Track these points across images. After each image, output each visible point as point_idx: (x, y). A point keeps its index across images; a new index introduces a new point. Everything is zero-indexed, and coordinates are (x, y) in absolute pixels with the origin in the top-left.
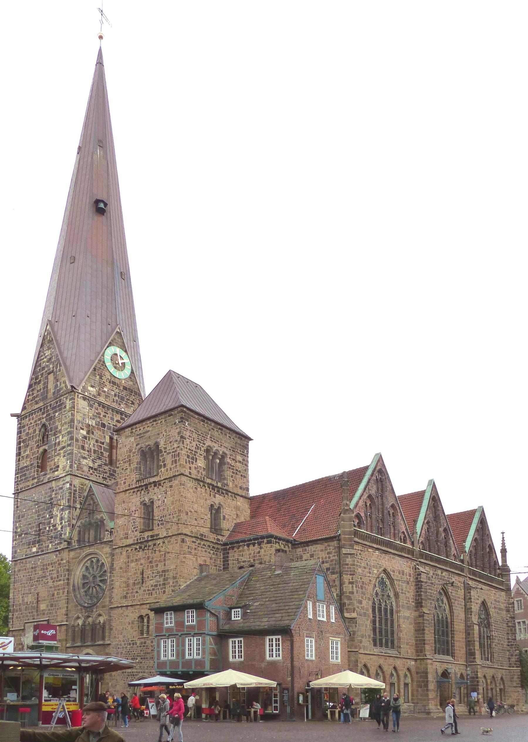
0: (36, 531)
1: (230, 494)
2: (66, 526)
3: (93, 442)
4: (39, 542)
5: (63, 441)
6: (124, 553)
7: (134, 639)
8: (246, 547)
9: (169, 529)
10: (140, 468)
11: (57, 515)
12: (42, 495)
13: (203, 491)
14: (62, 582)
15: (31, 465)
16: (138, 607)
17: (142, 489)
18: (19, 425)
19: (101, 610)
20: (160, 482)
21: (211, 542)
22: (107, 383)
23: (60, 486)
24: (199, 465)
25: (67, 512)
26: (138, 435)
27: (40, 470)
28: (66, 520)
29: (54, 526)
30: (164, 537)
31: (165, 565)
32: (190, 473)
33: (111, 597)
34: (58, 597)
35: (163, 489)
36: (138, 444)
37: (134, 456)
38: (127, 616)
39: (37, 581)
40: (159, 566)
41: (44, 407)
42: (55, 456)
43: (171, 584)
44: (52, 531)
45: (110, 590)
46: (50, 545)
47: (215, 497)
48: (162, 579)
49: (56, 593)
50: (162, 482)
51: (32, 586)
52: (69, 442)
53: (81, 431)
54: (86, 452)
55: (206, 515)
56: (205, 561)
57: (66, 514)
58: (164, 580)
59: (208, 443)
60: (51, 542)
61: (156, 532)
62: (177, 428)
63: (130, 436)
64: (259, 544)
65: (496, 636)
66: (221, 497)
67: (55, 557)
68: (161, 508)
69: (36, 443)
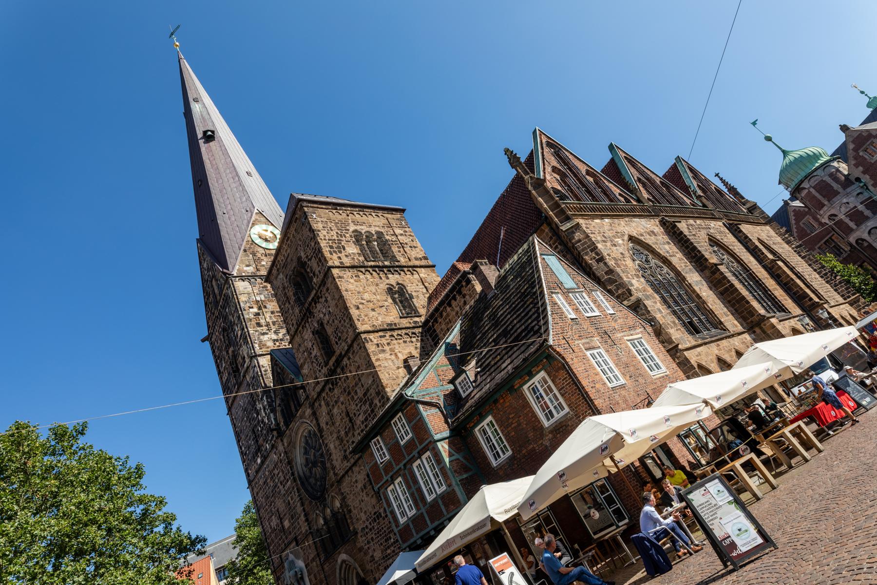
1: (406, 269)
3: (268, 315)
6: (323, 403)
7: (376, 510)
8: (448, 309)
13: (369, 276)
22: (263, 257)
30: (348, 351)
32: (341, 263)
33: (333, 468)
35: (324, 299)
38: (356, 481)
40: (358, 391)
43: (378, 404)
45: (329, 459)
47: (388, 278)
53: (251, 310)
55: (386, 301)
58: (370, 405)
59: (352, 228)
61: (338, 353)
64: (460, 292)
66: (397, 276)
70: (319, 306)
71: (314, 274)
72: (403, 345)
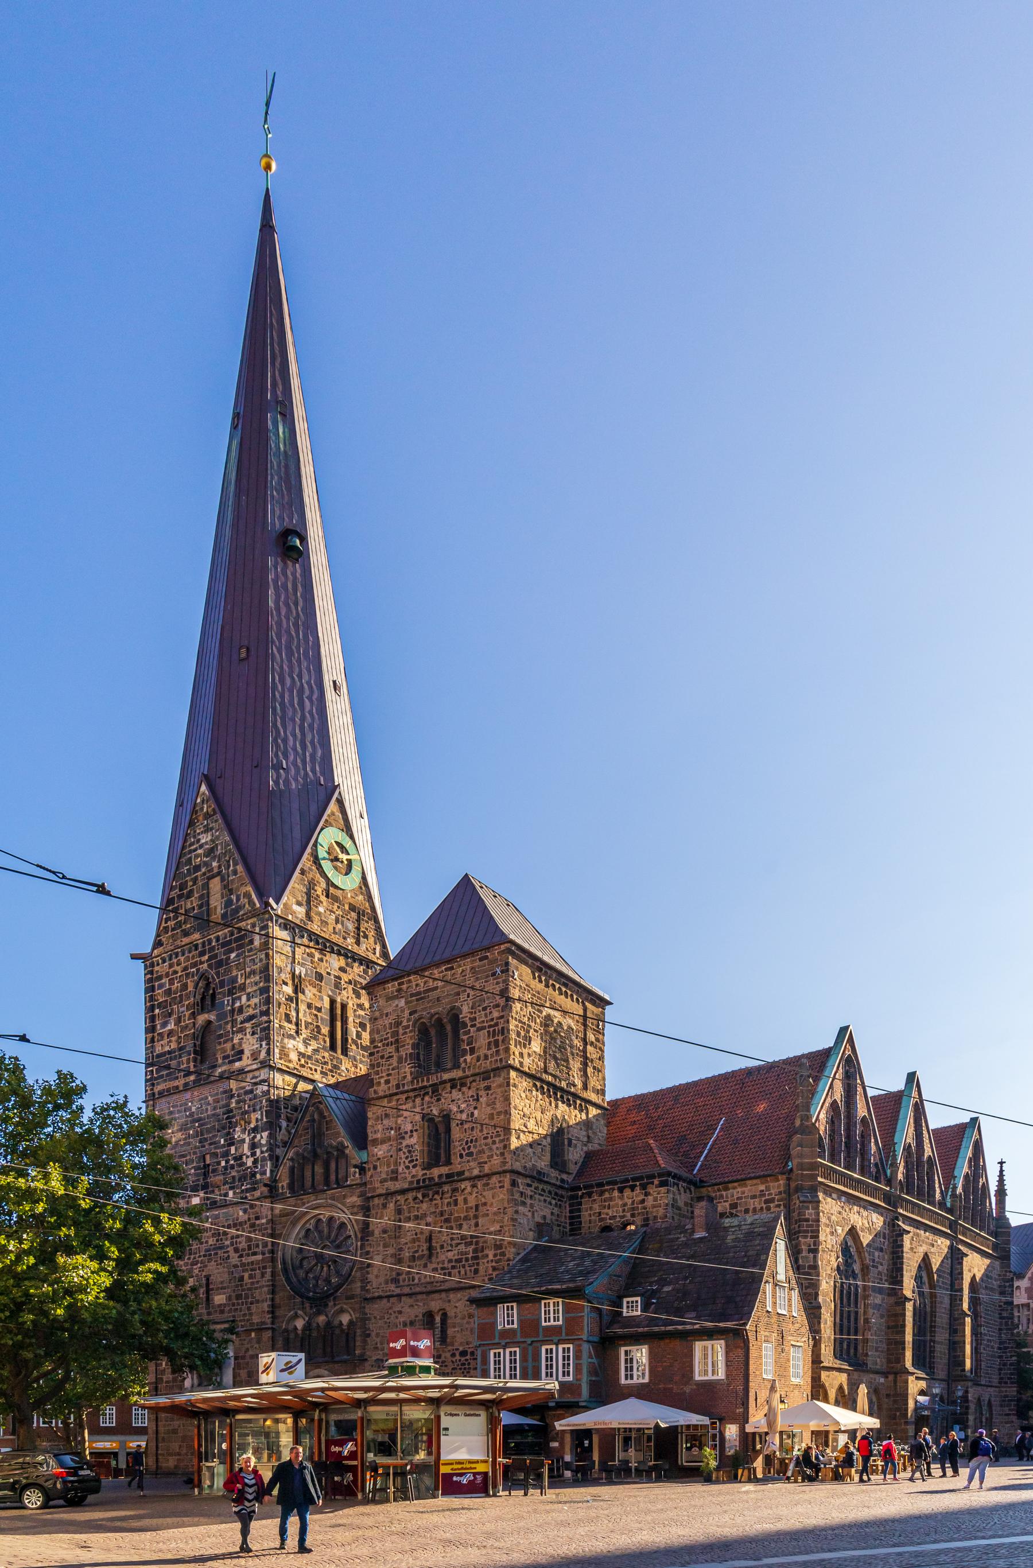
0: (196, 1168)
2: (264, 1159)
4: (205, 1187)
5: (249, 1006)
6: (392, 1205)
8: (616, 1193)
9: (486, 1163)
10: (418, 1054)
11: (243, 1141)
12: (209, 1104)
14: (259, 1257)
15: (180, 1049)
16: (424, 1296)
17: (427, 1093)
19: (346, 1304)
20: (463, 1081)
21: (554, 1185)
23: (248, 1088)
24: (534, 1049)
25: (265, 1134)
26: (412, 995)
27: (199, 1058)
28: (265, 1149)
29: (238, 1158)
30: (478, 1177)
31: (477, 1225)
32: (521, 1063)
34: (252, 1283)
36: (415, 1012)
37: (405, 1033)
39: (205, 1256)
41: (204, 943)
42: (233, 1033)
43: (491, 1257)
44: (232, 1167)
46: (231, 1193)
47: (557, 1107)
48: (471, 1249)
49: (246, 1275)
50: (468, 1081)
51: (193, 1264)
52: (264, 1008)
56: (544, 1217)
57: (263, 1137)
58: (475, 1251)
59: (546, 1011)
60: (231, 1188)
62: (498, 983)
63: (397, 997)
64: (644, 1187)
65: (985, 1335)
67: (241, 1213)
68: (466, 1126)
69: (188, 1009)
70: (455, 1094)
71: (472, 1051)
72: (542, 1204)
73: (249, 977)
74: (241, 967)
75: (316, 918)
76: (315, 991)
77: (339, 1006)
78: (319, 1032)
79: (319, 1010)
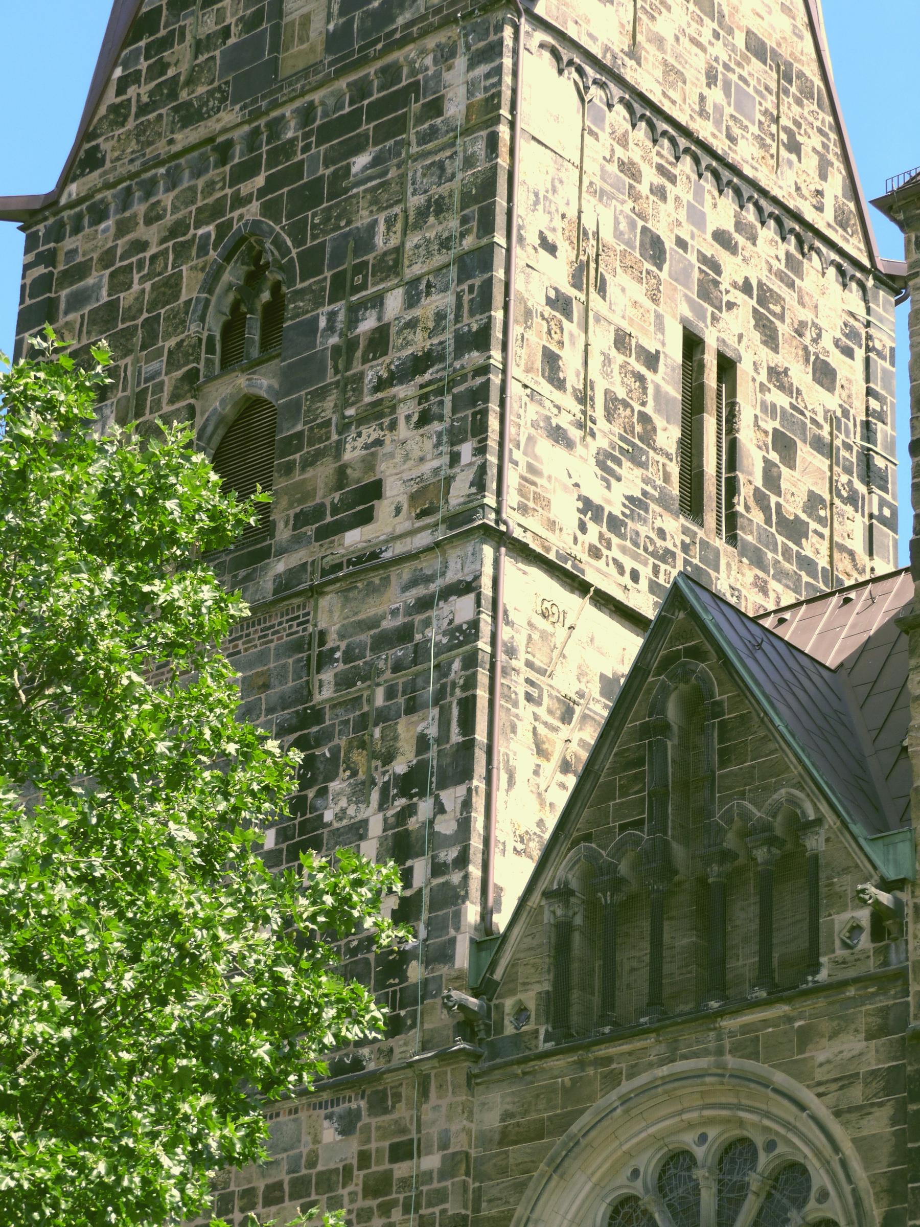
3: (601, 339)
5: (412, 324)
18: (41, 270)
23: (388, 624)
42: (344, 428)
54: (568, 401)
67: (329, 1134)
69: (172, 364)
73: (417, 226)
74: (385, 195)
75: (650, 52)
76: (637, 291)
77: (711, 361)
78: (648, 436)
79: (652, 360)
